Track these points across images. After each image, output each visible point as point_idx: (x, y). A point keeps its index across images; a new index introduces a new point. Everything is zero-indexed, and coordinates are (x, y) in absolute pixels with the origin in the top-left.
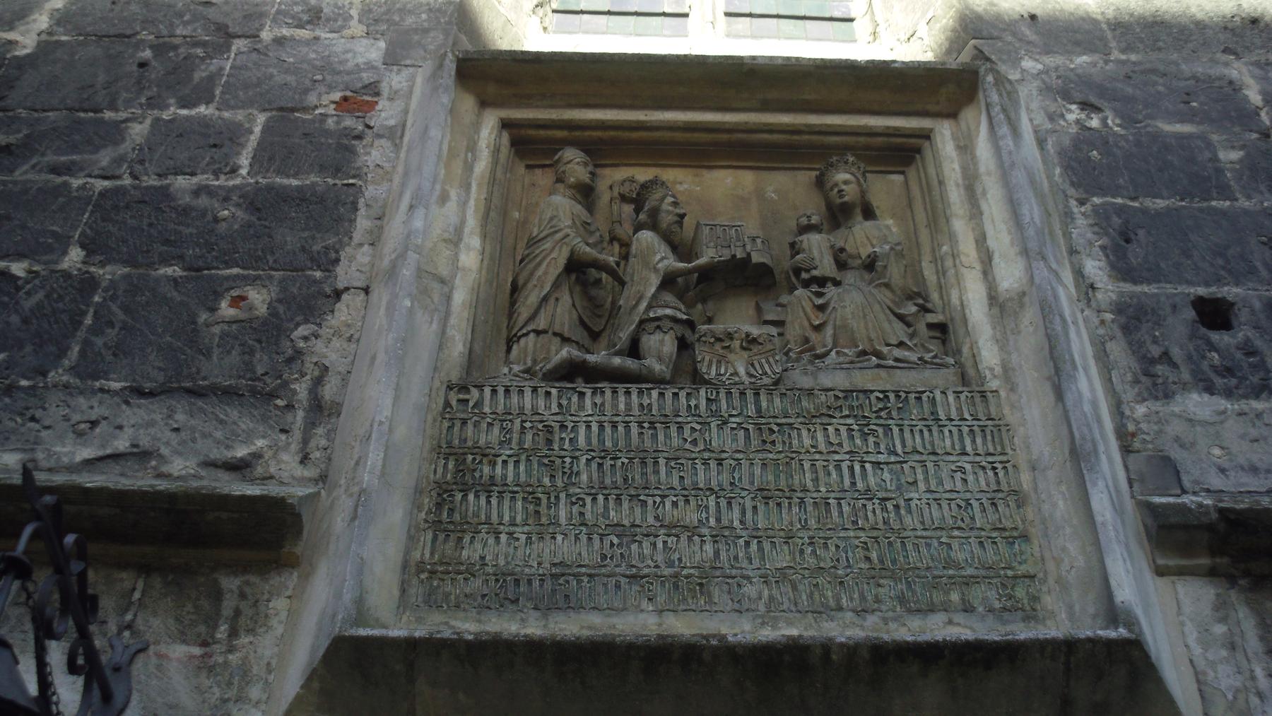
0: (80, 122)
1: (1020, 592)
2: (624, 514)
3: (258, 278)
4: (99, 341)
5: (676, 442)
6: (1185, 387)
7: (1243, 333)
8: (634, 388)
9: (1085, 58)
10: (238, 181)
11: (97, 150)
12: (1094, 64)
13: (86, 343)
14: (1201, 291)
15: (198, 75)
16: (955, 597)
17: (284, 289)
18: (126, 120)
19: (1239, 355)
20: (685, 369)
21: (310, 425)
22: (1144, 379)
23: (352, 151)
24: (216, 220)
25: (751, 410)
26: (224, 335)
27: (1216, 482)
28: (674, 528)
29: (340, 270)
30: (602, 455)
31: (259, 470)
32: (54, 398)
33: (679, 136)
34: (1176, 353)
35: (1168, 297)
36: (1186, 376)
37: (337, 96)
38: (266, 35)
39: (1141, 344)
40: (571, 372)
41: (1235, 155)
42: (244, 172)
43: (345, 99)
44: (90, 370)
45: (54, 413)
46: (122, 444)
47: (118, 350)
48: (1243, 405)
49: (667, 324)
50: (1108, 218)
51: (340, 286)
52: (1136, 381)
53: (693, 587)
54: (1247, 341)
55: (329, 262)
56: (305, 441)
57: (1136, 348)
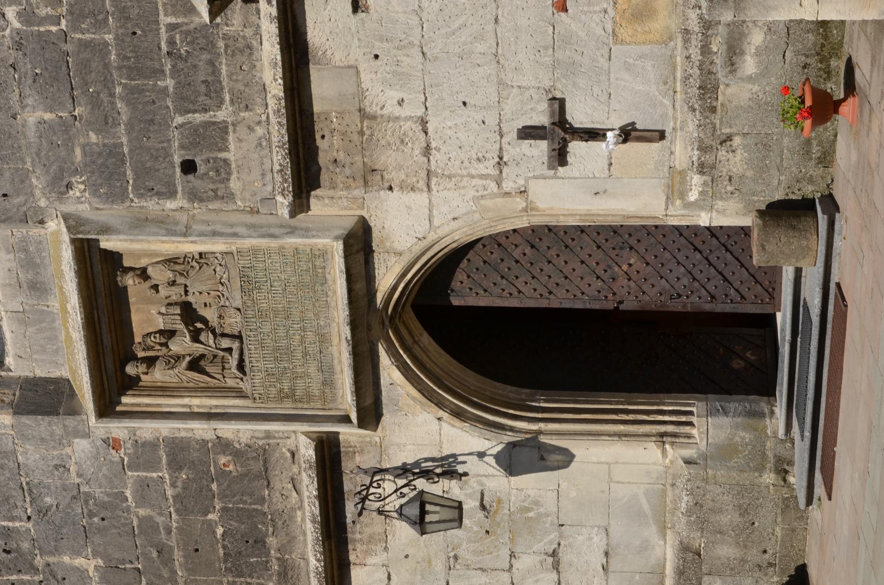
0: (141, 533)
1: (317, 253)
2: (299, 355)
3: (214, 462)
4: (249, 501)
5: (269, 341)
6: (227, 187)
7: (198, 160)
8: (246, 352)
9: (34, 180)
10: (167, 476)
11: (155, 522)
12: (38, 178)
13: (251, 504)
14: (178, 170)
15: (106, 499)
16: (320, 271)
17: (219, 453)
18: (138, 517)
19: (210, 165)
20: (239, 337)
21: (275, 438)
22: (225, 200)
23: (144, 444)
24: (188, 478)
25: (254, 320)
26: (241, 466)
27: (269, 188)
28: (302, 342)
29: (207, 439)
30: (276, 359)
31: (294, 449)
32: (274, 508)
33: (114, 334)
34: (211, 186)
35: (183, 182)
36: (223, 186)
37: (113, 452)
38: (78, 480)
39: (208, 197)
40: (241, 367)
41: (93, 137)
42: (160, 474)
43: (113, 448)
44: (262, 500)
45: (280, 506)
46: (290, 486)
47: (251, 495)
48: (234, 171)
49: (217, 341)
50: (141, 194)
51: (215, 437)
52: (227, 203)
53: (323, 339)
54: (202, 160)
55: (205, 442)
56: (282, 438)
57: (209, 199)
